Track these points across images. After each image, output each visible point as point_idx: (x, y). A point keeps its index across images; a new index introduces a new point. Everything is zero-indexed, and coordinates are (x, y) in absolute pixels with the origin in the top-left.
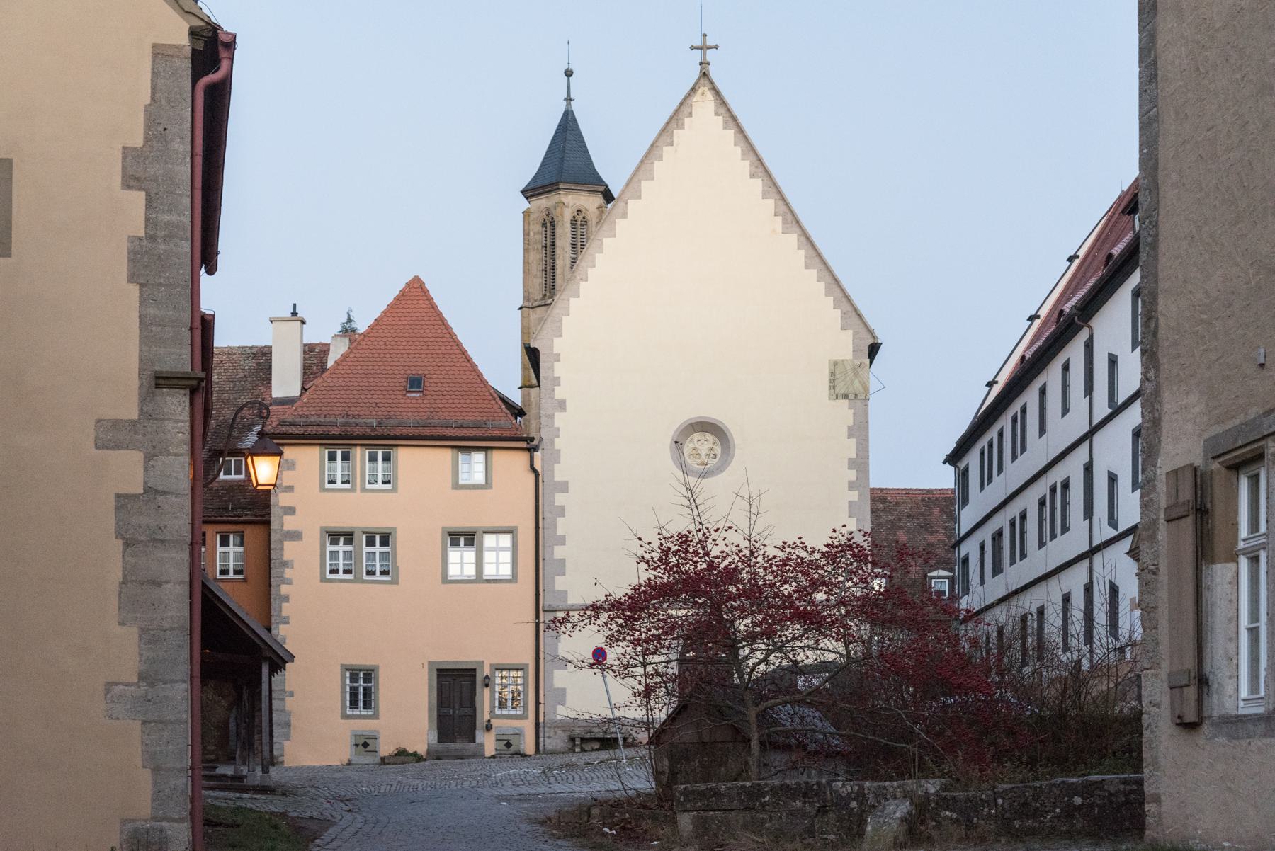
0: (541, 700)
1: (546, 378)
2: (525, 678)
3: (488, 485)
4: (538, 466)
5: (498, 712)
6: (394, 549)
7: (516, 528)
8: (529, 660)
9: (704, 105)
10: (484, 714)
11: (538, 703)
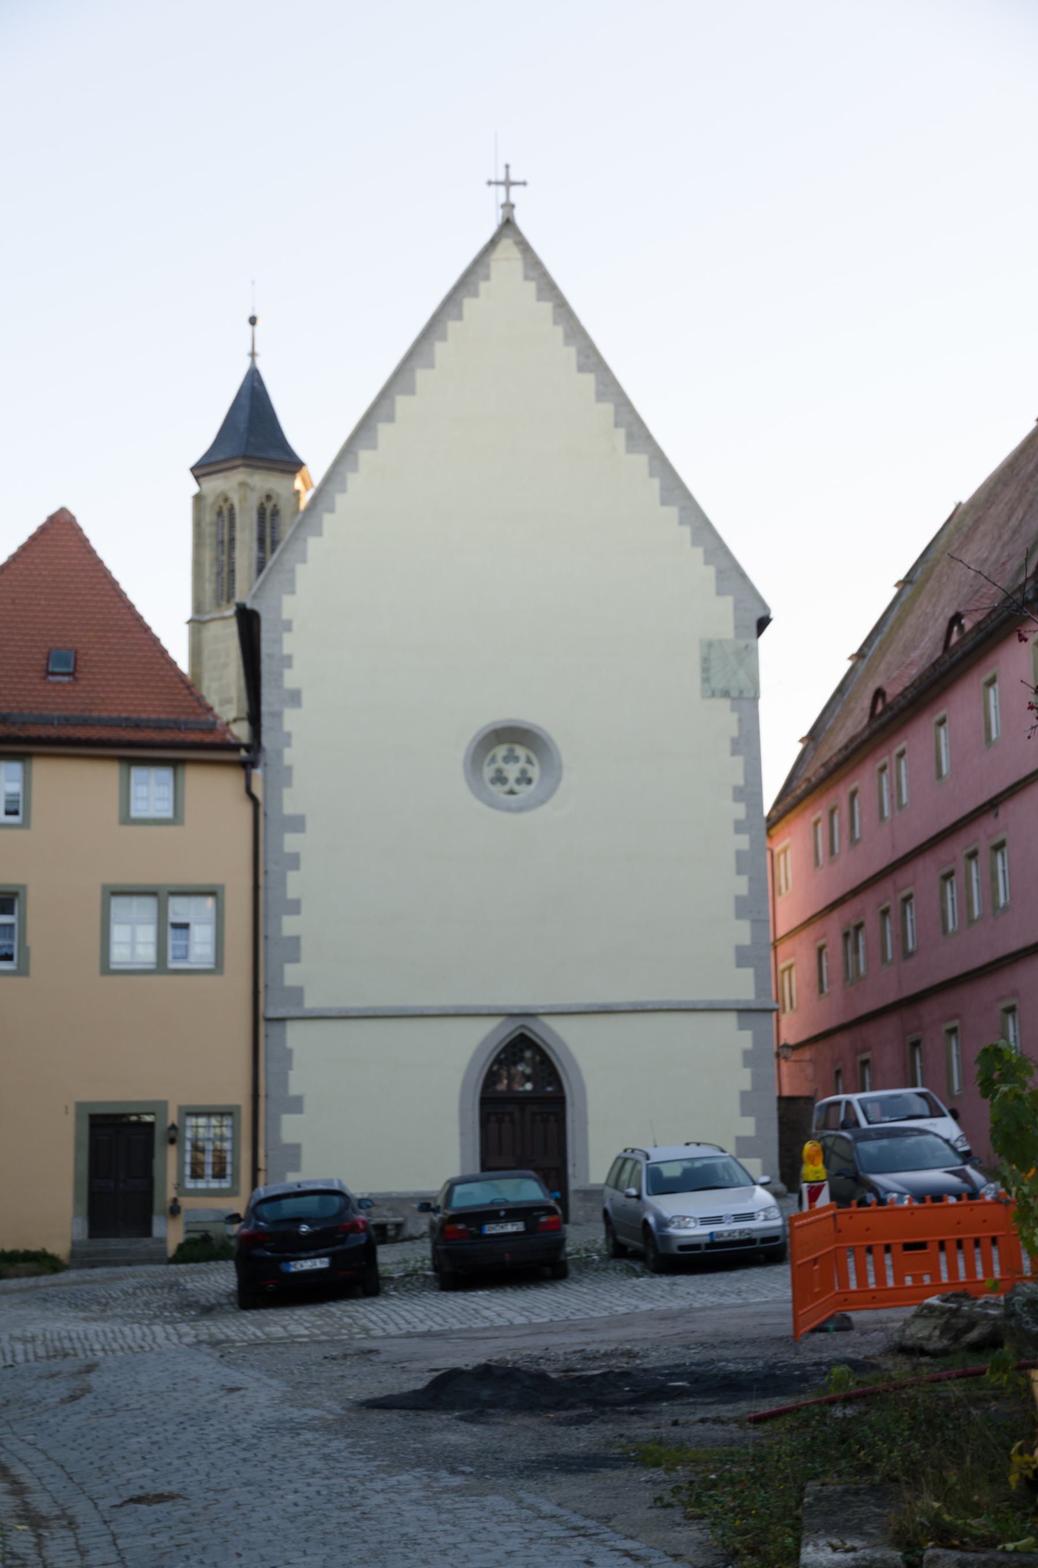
0: (262, 1164)
1: (270, 656)
2: (235, 1128)
3: (177, 819)
4: (257, 790)
5: (190, 1184)
6: (23, 919)
7: (222, 887)
8: (239, 1096)
9: (507, 262)
10: (167, 1189)
11: (255, 1170)
